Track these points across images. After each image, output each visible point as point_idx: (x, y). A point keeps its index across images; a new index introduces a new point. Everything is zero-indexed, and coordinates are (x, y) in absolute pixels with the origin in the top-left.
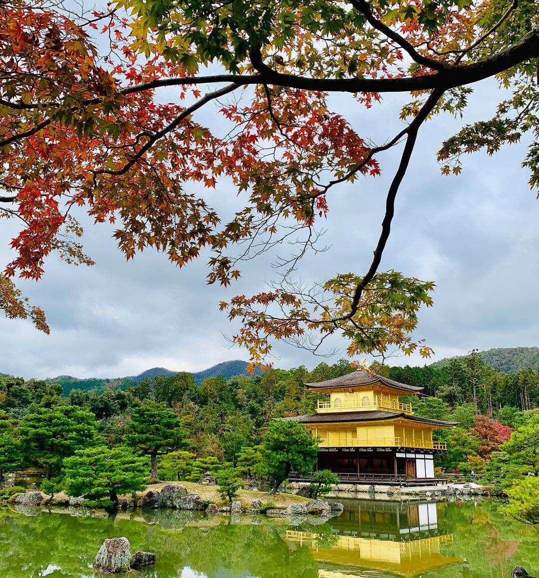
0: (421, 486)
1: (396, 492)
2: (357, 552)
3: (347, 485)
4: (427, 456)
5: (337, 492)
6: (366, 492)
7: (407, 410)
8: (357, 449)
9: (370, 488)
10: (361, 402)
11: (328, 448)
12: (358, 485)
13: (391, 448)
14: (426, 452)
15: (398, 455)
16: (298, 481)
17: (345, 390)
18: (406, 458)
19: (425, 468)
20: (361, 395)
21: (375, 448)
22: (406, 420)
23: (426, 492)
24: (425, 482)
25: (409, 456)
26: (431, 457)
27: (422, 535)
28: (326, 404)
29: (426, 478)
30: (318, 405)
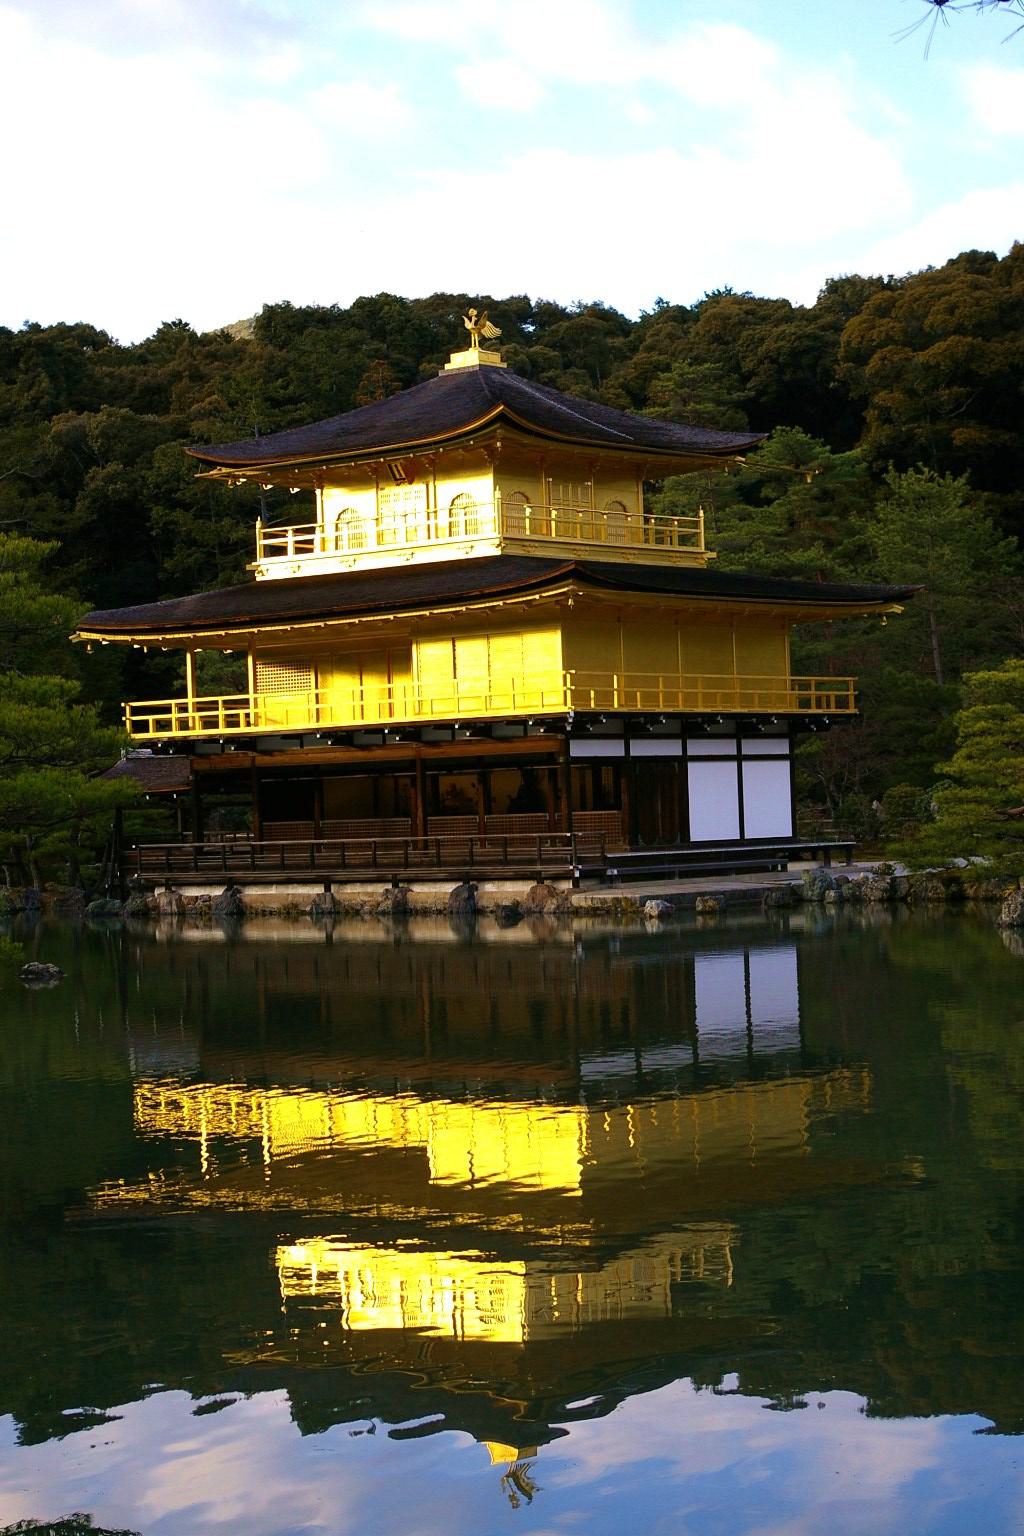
0: (684, 875)
1: (551, 905)
3: (370, 888)
4: (750, 747)
5: (327, 921)
6: (439, 912)
8: (412, 732)
9: (455, 894)
10: (443, 520)
11: (299, 737)
12: (417, 888)
13: (541, 720)
14: (745, 727)
15: (579, 749)
17: (375, 471)
19: (739, 800)
20: (447, 488)
21: (483, 728)
22: (602, 593)
23: (644, 900)
24: (718, 857)
25: (641, 749)
26: (782, 747)
27: (701, 1078)
29: (742, 841)
30: (261, 542)
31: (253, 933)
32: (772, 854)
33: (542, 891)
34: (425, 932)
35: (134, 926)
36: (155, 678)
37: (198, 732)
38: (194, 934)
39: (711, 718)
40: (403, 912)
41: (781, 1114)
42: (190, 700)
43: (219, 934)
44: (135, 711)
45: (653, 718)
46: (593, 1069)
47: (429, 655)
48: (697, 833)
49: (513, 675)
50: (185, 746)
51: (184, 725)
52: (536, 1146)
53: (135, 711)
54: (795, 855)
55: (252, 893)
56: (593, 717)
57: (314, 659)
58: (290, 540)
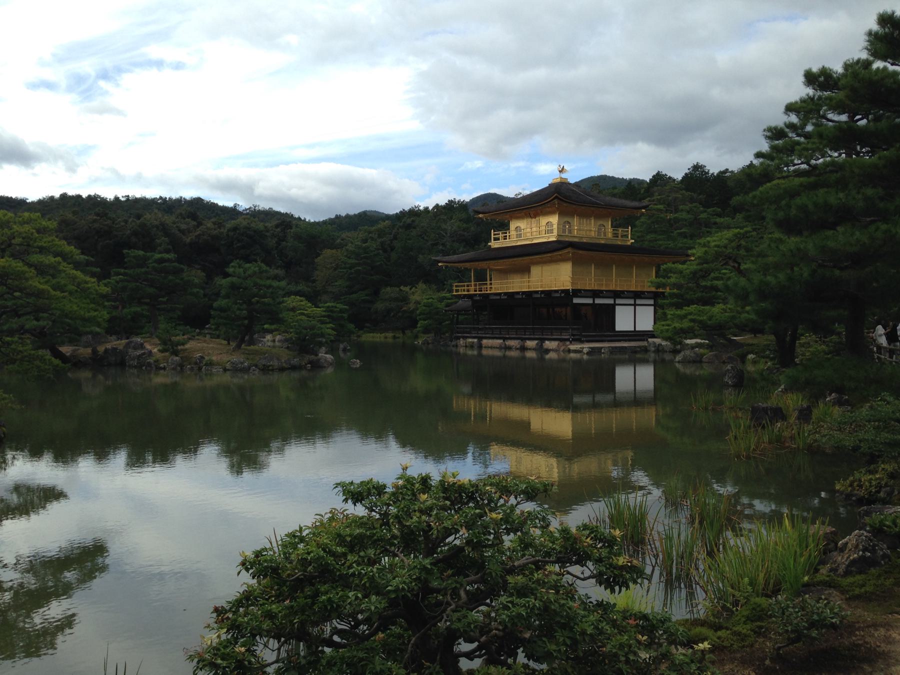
1: (562, 348)
2: (529, 423)
4: (638, 302)
7: (620, 238)
8: (529, 294)
11: (500, 294)
13: (563, 291)
14: (637, 295)
15: (576, 301)
16: (465, 338)
18: (594, 305)
20: (544, 220)
21: (548, 293)
22: (581, 252)
25: (598, 301)
26: (652, 302)
27: (617, 404)
28: (501, 236)
31: (484, 352)
32: (643, 335)
33: (561, 344)
34: (531, 354)
35: (454, 349)
36: (462, 276)
37: (472, 292)
38: (470, 352)
39: (623, 292)
40: (523, 349)
41: (636, 418)
42: (473, 283)
43: (475, 353)
44: (457, 286)
45: (601, 291)
46: (577, 400)
47: (536, 271)
48: (617, 329)
49: (558, 277)
50: (470, 297)
51: (468, 291)
52: (558, 423)
53: (457, 286)
54: (653, 336)
55: (485, 341)
56: (580, 291)
57: (506, 273)
58: (501, 236)
